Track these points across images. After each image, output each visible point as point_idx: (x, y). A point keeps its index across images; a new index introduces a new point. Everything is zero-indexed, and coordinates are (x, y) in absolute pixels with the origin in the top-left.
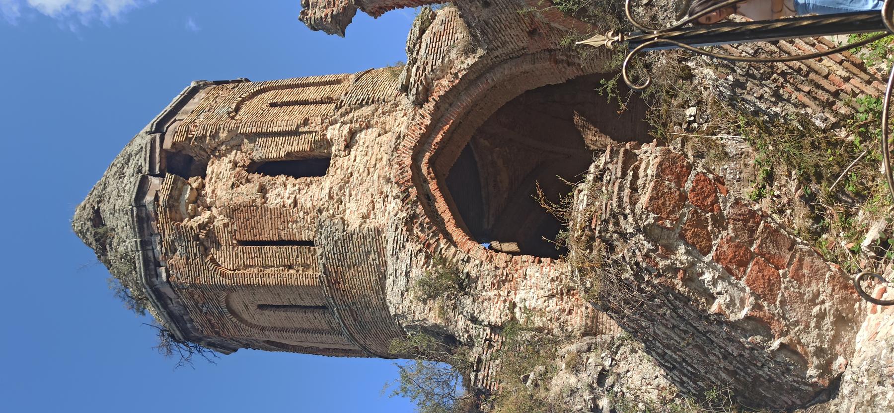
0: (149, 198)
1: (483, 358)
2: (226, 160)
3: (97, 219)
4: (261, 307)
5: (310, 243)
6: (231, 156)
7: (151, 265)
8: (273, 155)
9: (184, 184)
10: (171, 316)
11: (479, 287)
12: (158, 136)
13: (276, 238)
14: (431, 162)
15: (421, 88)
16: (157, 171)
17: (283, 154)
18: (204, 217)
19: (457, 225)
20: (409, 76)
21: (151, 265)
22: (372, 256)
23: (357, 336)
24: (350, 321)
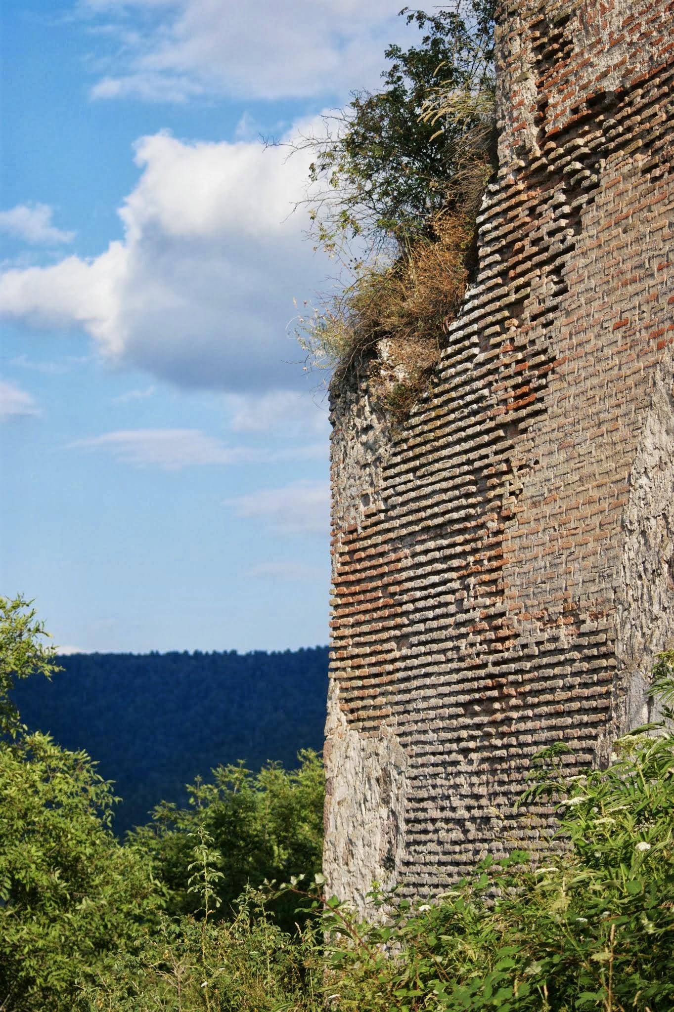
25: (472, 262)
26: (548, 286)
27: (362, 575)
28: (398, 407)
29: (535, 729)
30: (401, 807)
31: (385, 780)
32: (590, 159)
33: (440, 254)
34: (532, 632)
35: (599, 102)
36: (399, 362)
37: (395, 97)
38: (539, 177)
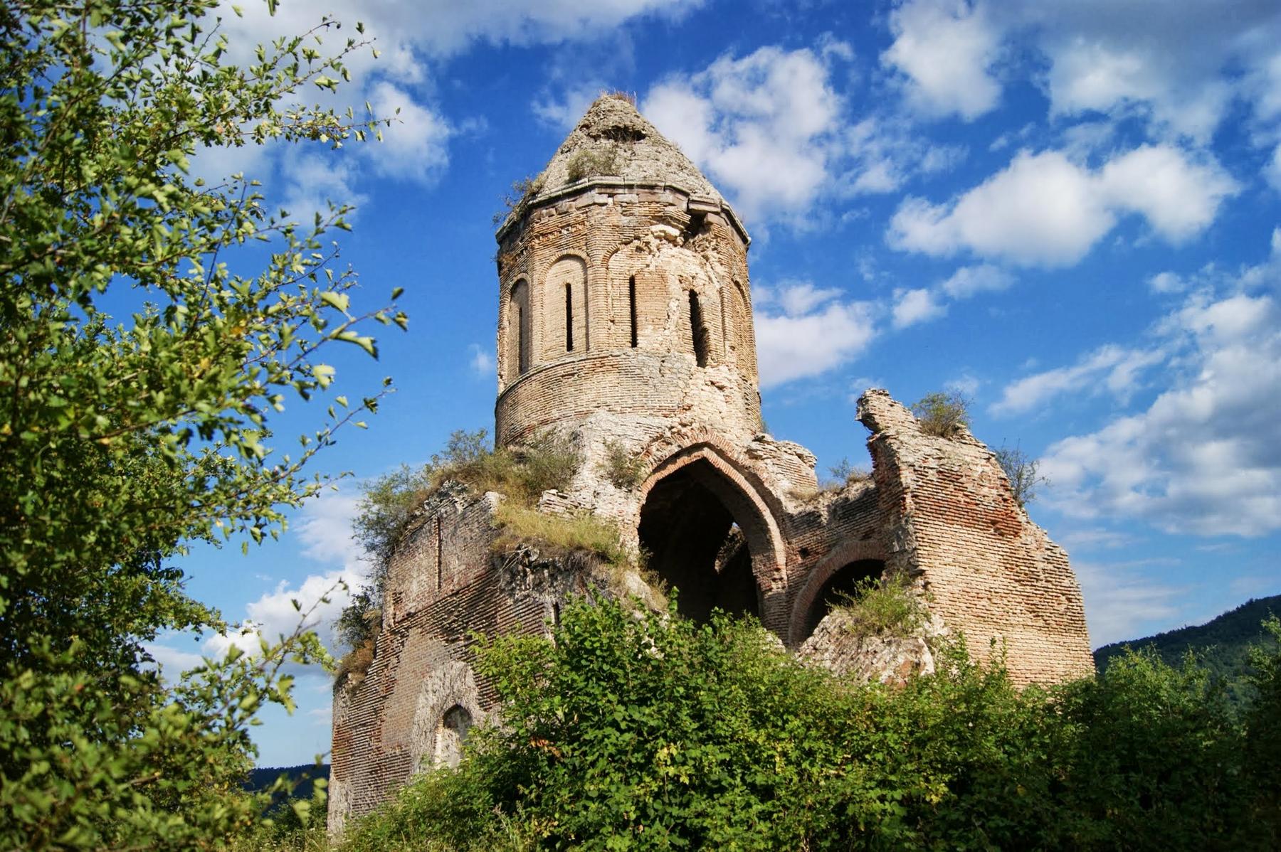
0: (668, 197)
2: (698, 269)
3: (639, 136)
4: (568, 287)
5: (634, 343)
6: (702, 275)
7: (610, 189)
8: (706, 316)
9: (681, 230)
10: (558, 198)
12: (718, 210)
13: (638, 311)
14: (704, 460)
15: (760, 453)
16: (692, 206)
17: (707, 325)
18: (653, 248)
19: (659, 483)
21: (610, 189)
22: (630, 401)
25: (375, 653)
26: (395, 661)
27: (342, 739)
28: (353, 691)
29: (389, 777)
30: (351, 802)
32: (407, 629)
33: (366, 651)
34: (389, 751)
35: (409, 614)
36: (353, 679)
37: (355, 607)
38: (393, 633)
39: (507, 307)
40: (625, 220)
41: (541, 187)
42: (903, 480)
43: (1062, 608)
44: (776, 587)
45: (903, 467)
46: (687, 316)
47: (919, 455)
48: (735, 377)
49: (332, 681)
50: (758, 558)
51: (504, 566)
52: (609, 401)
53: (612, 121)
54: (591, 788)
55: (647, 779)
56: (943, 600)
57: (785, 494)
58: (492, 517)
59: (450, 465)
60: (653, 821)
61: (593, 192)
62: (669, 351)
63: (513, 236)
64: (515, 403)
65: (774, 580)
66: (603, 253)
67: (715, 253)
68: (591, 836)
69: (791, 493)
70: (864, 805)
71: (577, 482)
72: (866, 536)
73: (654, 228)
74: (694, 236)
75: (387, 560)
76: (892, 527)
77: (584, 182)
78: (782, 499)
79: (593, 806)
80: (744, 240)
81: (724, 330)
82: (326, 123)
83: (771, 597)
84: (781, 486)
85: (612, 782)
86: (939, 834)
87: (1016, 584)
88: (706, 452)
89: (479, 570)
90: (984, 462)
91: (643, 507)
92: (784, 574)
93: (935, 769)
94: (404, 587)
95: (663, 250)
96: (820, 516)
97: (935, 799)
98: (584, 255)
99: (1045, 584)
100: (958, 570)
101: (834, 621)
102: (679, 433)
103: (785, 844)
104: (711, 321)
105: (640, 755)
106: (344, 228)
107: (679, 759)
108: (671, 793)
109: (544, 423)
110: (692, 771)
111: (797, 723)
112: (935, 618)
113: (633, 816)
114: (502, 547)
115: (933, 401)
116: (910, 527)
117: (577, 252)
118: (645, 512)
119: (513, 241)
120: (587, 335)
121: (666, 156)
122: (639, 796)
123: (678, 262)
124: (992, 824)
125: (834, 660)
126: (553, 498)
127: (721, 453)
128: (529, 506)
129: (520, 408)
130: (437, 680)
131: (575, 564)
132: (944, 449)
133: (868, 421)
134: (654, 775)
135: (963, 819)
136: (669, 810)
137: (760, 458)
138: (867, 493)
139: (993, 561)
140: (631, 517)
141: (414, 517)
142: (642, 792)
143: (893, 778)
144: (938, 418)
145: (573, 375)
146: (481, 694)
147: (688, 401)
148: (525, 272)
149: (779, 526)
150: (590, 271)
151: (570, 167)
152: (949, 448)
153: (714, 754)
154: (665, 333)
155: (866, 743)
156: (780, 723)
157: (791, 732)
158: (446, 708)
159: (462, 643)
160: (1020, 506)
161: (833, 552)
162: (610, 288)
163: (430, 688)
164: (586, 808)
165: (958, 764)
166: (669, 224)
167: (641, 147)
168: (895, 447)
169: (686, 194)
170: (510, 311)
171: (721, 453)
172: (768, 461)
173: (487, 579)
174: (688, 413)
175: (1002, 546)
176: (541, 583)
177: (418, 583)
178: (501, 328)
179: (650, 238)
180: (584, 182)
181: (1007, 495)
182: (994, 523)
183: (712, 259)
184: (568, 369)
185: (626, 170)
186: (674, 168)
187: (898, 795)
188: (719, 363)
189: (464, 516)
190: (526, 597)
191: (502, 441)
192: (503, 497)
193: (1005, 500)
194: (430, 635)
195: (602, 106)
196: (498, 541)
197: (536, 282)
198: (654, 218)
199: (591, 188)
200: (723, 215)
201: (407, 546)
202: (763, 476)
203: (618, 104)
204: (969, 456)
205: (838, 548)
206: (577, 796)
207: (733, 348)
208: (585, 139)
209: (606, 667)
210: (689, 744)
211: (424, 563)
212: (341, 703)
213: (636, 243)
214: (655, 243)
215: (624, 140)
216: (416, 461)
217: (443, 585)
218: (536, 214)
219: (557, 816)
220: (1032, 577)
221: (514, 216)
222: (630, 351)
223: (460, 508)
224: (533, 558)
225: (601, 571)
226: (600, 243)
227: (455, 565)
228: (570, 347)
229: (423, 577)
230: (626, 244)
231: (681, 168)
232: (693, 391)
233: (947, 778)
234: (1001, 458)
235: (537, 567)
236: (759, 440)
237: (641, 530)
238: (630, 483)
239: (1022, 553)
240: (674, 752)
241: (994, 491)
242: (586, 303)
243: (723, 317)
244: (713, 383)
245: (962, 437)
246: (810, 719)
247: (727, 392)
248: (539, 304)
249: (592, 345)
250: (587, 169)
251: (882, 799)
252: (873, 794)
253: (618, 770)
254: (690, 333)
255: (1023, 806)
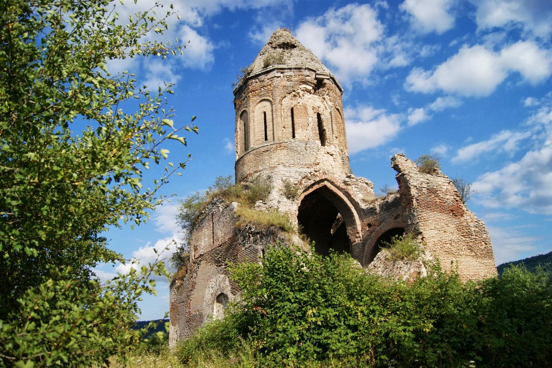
1: (266, 205)
2: (321, 104)
3: (293, 46)
4: (265, 113)
5: (294, 137)
6: (322, 106)
7: (282, 70)
8: (325, 124)
9: (313, 87)
10: (259, 75)
11: (289, 205)
12: (329, 77)
14: (325, 186)
15: (349, 183)
16: (317, 76)
17: (325, 128)
18: (301, 95)
19: (306, 197)
20: (353, 178)
21: (282, 70)
23: (255, 151)
24: (262, 149)
25: (187, 272)
27: (174, 307)
28: (178, 288)
30: (179, 335)
31: (176, 331)
32: (200, 261)
33: (183, 271)
34: (194, 313)
35: (201, 255)
36: (178, 283)
37: (178, 253)
38: (194, 263)
39: (239, 123)
40: (288, 83)
41: (252, 70)
42: (412, 193)
43: (483, 247)
44: (357, 240)
45: (412, 187)
46: (316, 124)
47: (419, 182)
48: (338, 150)
49: (169, 284)
50: (349, 228)
51: (240, 234)
52: (283, 162)
53: (282, 40)
54: (280, 327)
55: (303, 323)
56: (430, 245)
57: (360, 200)
58: (235, 213)
59: (216, 191)
60: (306, 341)
61: (274, 72)
62: (309, 139)
63: (241, 92)
64: (243, 164)
65: (357, 237)
66: (279, 98)
67: (328, 97)
68: (280, 347)
69: (363, 200)
70: (397, 333)
71: (271, 197)
72: (396, 218)
73: (301, 86)
74: (318, 89)
75: (191, 232)
76: (407, 214)
77: (270, 68)
78: (359, 202)
79: (281, 335)
80: (340, 90)
81: (332, 130)
82: (159, 48)
83: (355, 245)
84: (358, 197)
85: (288, 325)
86: (429, 345)
87: (462, 237)
88: (326, 183)
89: (230, 235)
90: (447, 184)
91: (299, 207)
92: (361, 235)
93: (427, 317)
94: (199, 243)
95: (305, 96)
96: (376, 209)
97: (428, 330)
98: (271, 99)
99: (475, 237)
100: (437, 232)
101: (383, 255)
102: (314, 175)
103: (363, 350)
104: (327, 126)
105: (300, 313)
106: (170, 92)
107: (317, 314)
108: (314, 329)
109: (256, 172)
110: (322, 320)
111: (367, 298)
112: (427, 253)
113: (298, 339)
114: (239, 226)
115: (425, 158)
116: (415, 213)
117: (268, 98)
118: (300, 209)
119: (240, 94)
120: (273, 134)
121: (305, 55)
122: (300, 330)
123: (312, 101)
124: (452, 341)
125: (383, 272)
126: (260, 204)
127: (332, 183)
128: (250, 208)
129: (245, 166)
130: (213, 283)
131: (271, 232)
132: (430, 179)
133: (396, 168)
134: (306, 321)
135: (440, 339)
136: (313, 336)
137: (349, 185)
138: (396, 199)
139: (452, 228)
140: (294, 211)
141: (202, 213)
142: (301, 328)
143: (409, 321)
144: (427, 165)
145: (268, 151)
146: (232, 288)
147: (318, 161)
148: (246, 107)
149: (358, 214)
150: (274, 106)
151: (264, 61)
152: (432, 179)
153: (332, 312)
154: (307, 132)
155: (397, 307)
156: (360, 298)
157: (365, 302)
158: (217, 294)
159: (223, 267)
160: (463, 203)
161: (382, 224)
162: (283, 113)
163: (210, 286)
164: (278, 336)
165: (438, 315)
166: (307, 84)
167: (295, 51)
168: (408, 179)
169: (315, 71)
170: (240, 124)
171: (332, 183)
172: (353, 186)
173: (233, 239)
174: (318, 166)
175: (456, 221)
176: (256, 240)
177: (205, 241)
178: (236, 131)
179: (299, 91)
180: (270, 68)
181: (458, 199)
182: (452, 211)
183: (326, 99)
184: (265, 148)
185: (289, 62)
186: (309, 60)
187: (411, 328)
188: (331, 144)
189: (223, 213)
190: (250, 246)
191: (238, 181)
192: (239, 204)
193: (457, 201)
194: (210, 264)
195: (277, 34)
196: (237, 223)
197: (251, 111)
198: (301, 82)
199: (273, 70)
200: (331, 80)
201: (199, 226)
202: (351, 192)
203: (284, 33)
204: (441, 182)
205: (384, 223)
206: (274, 331)
207: (336, 137)
208: (270, 49)
209: (285, 276)
210: (321, 308)
211: (207, 233)
212: (173, 293)
213: (294, 93)
214: (301, 93)
215: (287, 49)
216: (202, 190)
217: (215, 242)
218: (250, 82)
219: (265, 339)
220: (469, 234)
221: (241, 83)
222: (292, 140)
223: (221, 209)
224: (253, 230)
225: (282, 235)
226: (278, 93)
227: (220, 234)
228: (266, 139)
229: (206, 239)
230: (289, 94)
231: (312, 60)
232: (320, 156)
233: (432, 321)
234: (455, 183)
235: (254, 234)
236: (349, 177)
237: (299, 217)
238: (293, 197)
239: (465, 224)
240: (315, 311)
241: (452, 197)
242: (273, 120)
243: (332, 124)
244: (328, 153)
245: (437, 174)
246: (373, 297)
247: (334, 156)
248: (252, 121)
249: (275, 138)
250: (271, 62)
251: (405, 331)
252: (400, 328)
253: (291, 319)
254: (318, 132)
255: (466, 333)
